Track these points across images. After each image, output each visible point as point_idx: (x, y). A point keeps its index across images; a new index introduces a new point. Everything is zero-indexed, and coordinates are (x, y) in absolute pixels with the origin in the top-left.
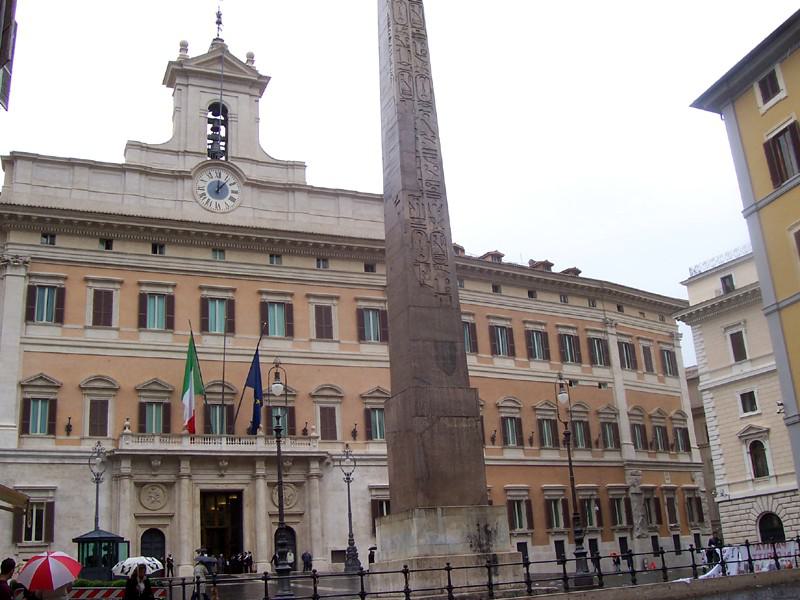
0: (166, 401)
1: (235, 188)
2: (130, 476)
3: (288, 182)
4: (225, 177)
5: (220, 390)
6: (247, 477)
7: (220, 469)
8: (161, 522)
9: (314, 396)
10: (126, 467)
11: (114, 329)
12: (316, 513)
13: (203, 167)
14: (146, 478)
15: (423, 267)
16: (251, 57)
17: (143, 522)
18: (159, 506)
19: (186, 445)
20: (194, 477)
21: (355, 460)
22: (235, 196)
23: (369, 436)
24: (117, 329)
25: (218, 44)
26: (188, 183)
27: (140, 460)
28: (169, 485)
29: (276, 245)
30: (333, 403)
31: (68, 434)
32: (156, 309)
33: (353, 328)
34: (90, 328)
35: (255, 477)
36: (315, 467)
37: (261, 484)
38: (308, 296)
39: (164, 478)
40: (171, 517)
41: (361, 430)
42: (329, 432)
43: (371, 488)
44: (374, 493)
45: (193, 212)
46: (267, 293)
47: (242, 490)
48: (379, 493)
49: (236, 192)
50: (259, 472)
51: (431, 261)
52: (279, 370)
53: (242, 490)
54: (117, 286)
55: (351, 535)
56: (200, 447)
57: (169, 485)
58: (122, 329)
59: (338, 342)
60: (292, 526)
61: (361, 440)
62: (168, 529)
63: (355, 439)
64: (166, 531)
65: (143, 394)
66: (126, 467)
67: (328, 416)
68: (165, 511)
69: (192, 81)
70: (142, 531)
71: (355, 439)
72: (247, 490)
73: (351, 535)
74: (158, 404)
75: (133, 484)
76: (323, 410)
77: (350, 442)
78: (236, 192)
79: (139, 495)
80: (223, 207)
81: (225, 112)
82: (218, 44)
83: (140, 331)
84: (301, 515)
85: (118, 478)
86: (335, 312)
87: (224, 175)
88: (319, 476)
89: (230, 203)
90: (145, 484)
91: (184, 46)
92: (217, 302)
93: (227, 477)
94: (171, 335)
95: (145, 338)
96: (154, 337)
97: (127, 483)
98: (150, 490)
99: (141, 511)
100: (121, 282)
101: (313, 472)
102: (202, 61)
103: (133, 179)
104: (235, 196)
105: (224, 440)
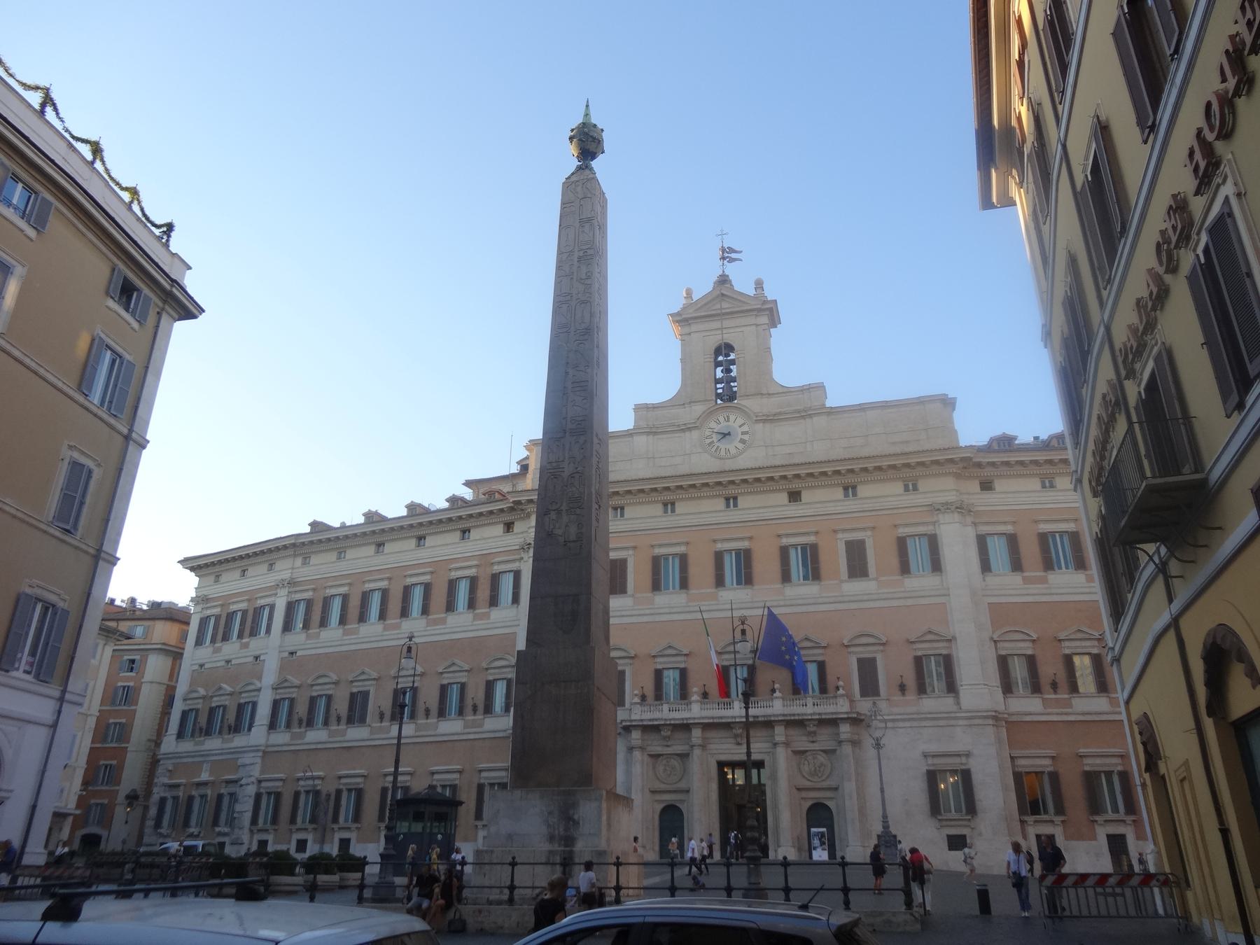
0: (682, 666)
1: (745, 428)
2: (642, 748)
3: (806, 405)
4: (735, 422)
5: (731, 648)
9: (847, 646)
10: (636, 735)
12: (850, 787)
13: (709, 414)
14: (659, 750)
15: (553, 515)
16: (759, 285)
17: (658, 797)
19: (696, 711)
21: (885, 721)
22: (746, 437)
23: (922, 689)
25: (723, 280)
26: (695, 434)
27: (651, 729)
28: (684, 757)
29: (793, 482)
30: (875, 652)
32: (672, 572)
33: (895, 562)
35: (775, 745)
36: (845, 729)
37: (781, 753)
39: (679, 748)
40: (688, 791)
41: (911, 681)
42: (869, 686)
43: (925, 756)
44: (930, 761)
45: (703, 462)
48: (937, 761)
49: (746, 433)
50: (778, 739)
51: (564, 507)
52: (746, 627)
54: (631, 552)
55: (885, 816)
56: (715, 712)
57: (684, 757)
59: (876, 579)
61: (911, 696)
63: (903, 694)
64: (683, 807)
65: (659, 660)
66: (636, 735)
67: (868, 669)
68: (682, 785)
69: (694, 328)
70: (659, 807)
71: (903, 694)
73: (885, 816)
75: (646, 758)
76: (860, 661)
77: (898, 698)
78: (746, 433)
79: (654, 768)
80: (733, 451)
81: (729, 348)
82: (723, 280)
84: (836, 789)
85: (631, 749)
87: (732, 418)
88: (855, 743)
89: (741, 446)
90: (659, 756)
91: (689, 293)
95: (661, 599)
96: (671, 602)
97: (637, 754)
99: (659, 786)
100: (635, 548)
101: (843, 737)
102: (708, 300)
103: (641, 441)
104: (746, 437)
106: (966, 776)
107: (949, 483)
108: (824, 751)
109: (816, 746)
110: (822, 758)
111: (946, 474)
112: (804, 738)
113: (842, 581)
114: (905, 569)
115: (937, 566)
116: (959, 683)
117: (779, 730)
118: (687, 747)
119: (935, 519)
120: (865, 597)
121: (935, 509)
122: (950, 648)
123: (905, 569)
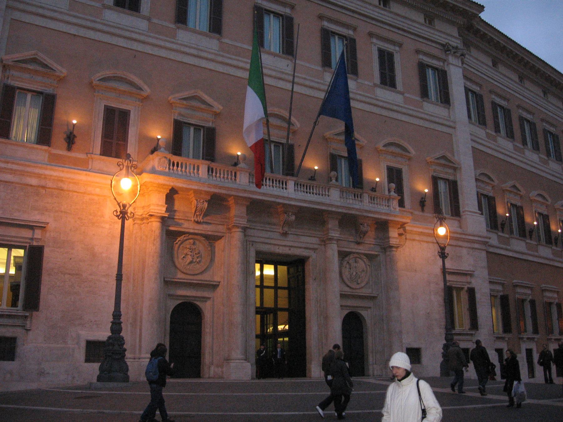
6: (315, 240)
7: (287, 223)
8: (199, 293)
11: (144, 18)
18: (198, 268)
20: (250, 232)
24: (149, 19)
31: (69, 149)
34: (109, 8)
35: (325, 241)
37: (333, 251)
38: (371, 35)
46: (330, 20)
47: (308, 258)
53: (308, 258)
58: (155, 21)
59: (402, 93)
60: (363, 313)
62: (209, 303)
64: (206, 308)
68: (206, 277)
70: (172, 304)
71: (423, 210)
72: (313, 255)
74: (197, 128)
83: (178, 28)
84: (373, 298)
86: (397, 59)
92: (272, 15)
93: (291, 237)
94: (215, 42)
95: (183, 36)
98: (187, 244)
105: (291, 185)
106: (471, 292)
107: (454, 32)
108: (367, 255)
109: (362, 249)
110: (361, 264)
111: (453, 23)
112: (351, 239)
113: (375, 85)
114: (424, 93)
115: (445, 99)
116: (461, 209)
117: (332, 224)
118: (222, 228)
119: (444, 57)
120: (395, 108)
121: (446, 48)
122: (455, 175)
123: (424, 93)
